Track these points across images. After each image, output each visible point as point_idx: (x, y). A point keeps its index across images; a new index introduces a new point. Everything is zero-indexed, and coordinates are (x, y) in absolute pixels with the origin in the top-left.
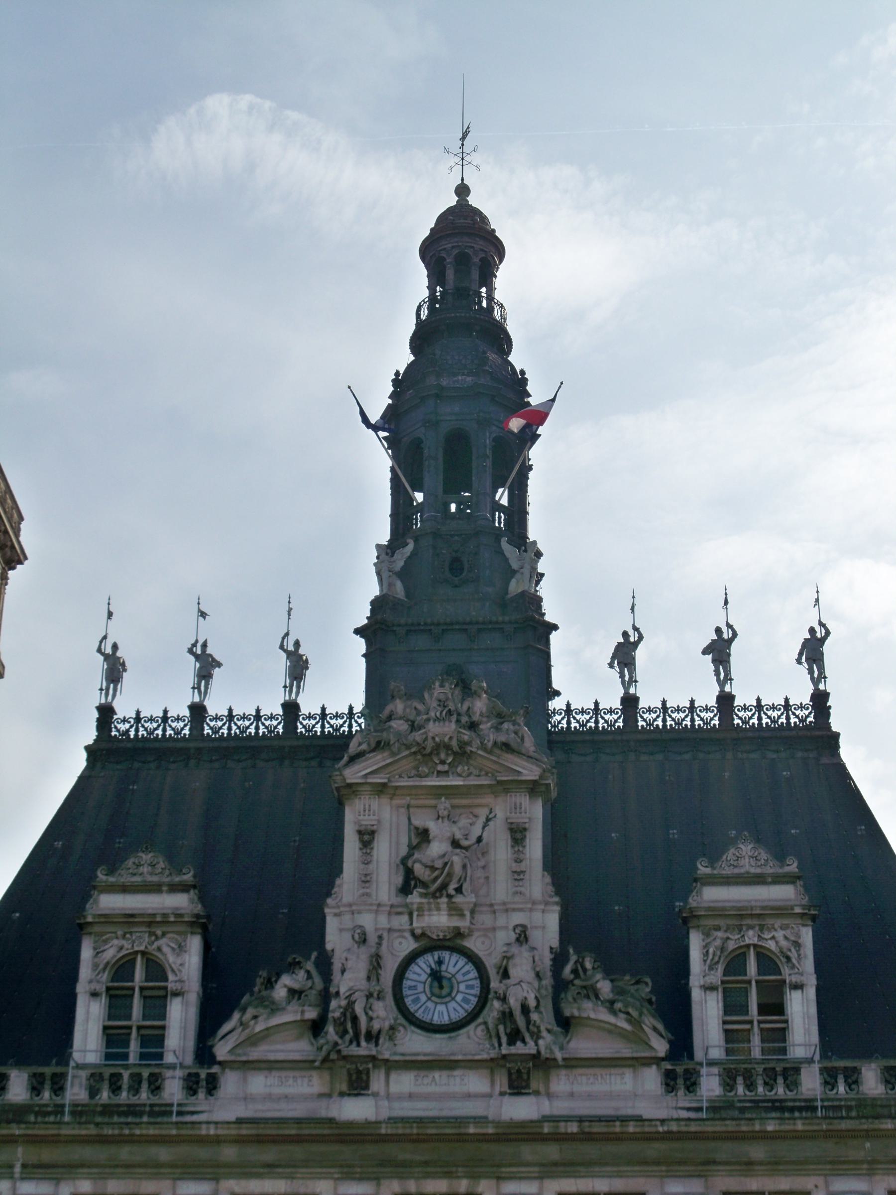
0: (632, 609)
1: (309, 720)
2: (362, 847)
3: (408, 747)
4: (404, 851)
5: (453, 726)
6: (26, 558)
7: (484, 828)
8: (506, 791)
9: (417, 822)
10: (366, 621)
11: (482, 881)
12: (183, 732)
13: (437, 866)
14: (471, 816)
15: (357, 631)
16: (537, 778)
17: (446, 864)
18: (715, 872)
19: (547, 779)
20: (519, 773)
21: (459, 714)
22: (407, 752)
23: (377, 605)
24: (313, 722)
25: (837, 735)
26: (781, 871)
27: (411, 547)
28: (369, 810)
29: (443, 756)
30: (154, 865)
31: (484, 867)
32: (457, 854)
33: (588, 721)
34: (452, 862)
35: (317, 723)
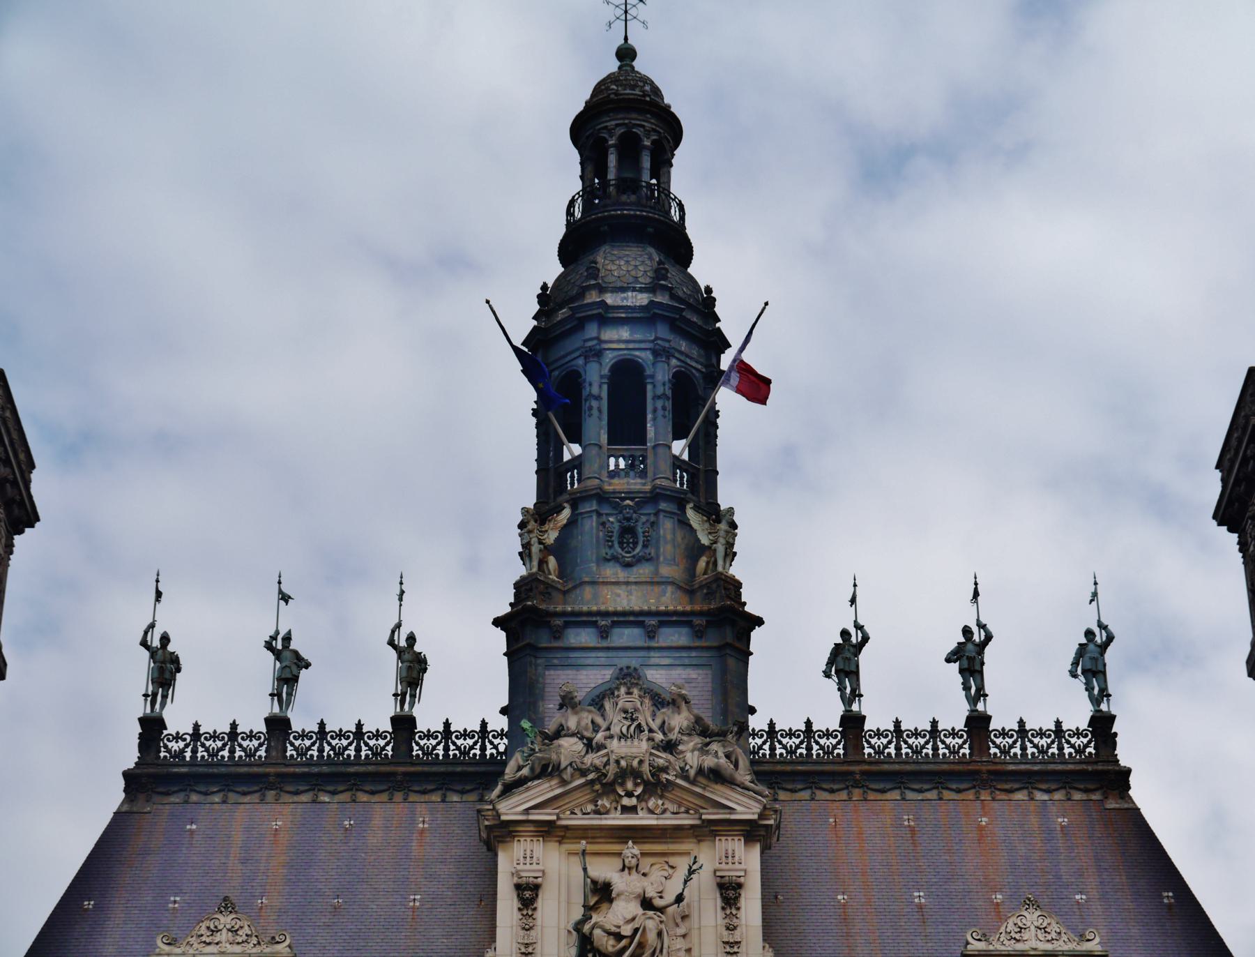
0: (853, 601)
1: (428, 740)
2: (520, 906)
3: (583, 773)
4: (578, 913)
5: (644, 745)
6: (38, 519)
7: (686, 882)
8: (714, 835)
10: (509, 609)
11: (682, 953)
12: (258, 754)
13: (623, 933)
14: (667, 867)
15: (497, 622)
16: (755, 817)
17: (636, 930)
18: (991, 948)
19: (769, 819)
21: (651, 731)
22: (581, 781)
23: (522, 588)
24: (434, 742)
25: (1128, 772)
26: (1079, 948)
27: (566, 513)
29: (630, 785)
30: (237, 930)
31: (684, 936)
32: (650, 918)
33: (798, 747)
34: (644, 929)
35: (438, 744)
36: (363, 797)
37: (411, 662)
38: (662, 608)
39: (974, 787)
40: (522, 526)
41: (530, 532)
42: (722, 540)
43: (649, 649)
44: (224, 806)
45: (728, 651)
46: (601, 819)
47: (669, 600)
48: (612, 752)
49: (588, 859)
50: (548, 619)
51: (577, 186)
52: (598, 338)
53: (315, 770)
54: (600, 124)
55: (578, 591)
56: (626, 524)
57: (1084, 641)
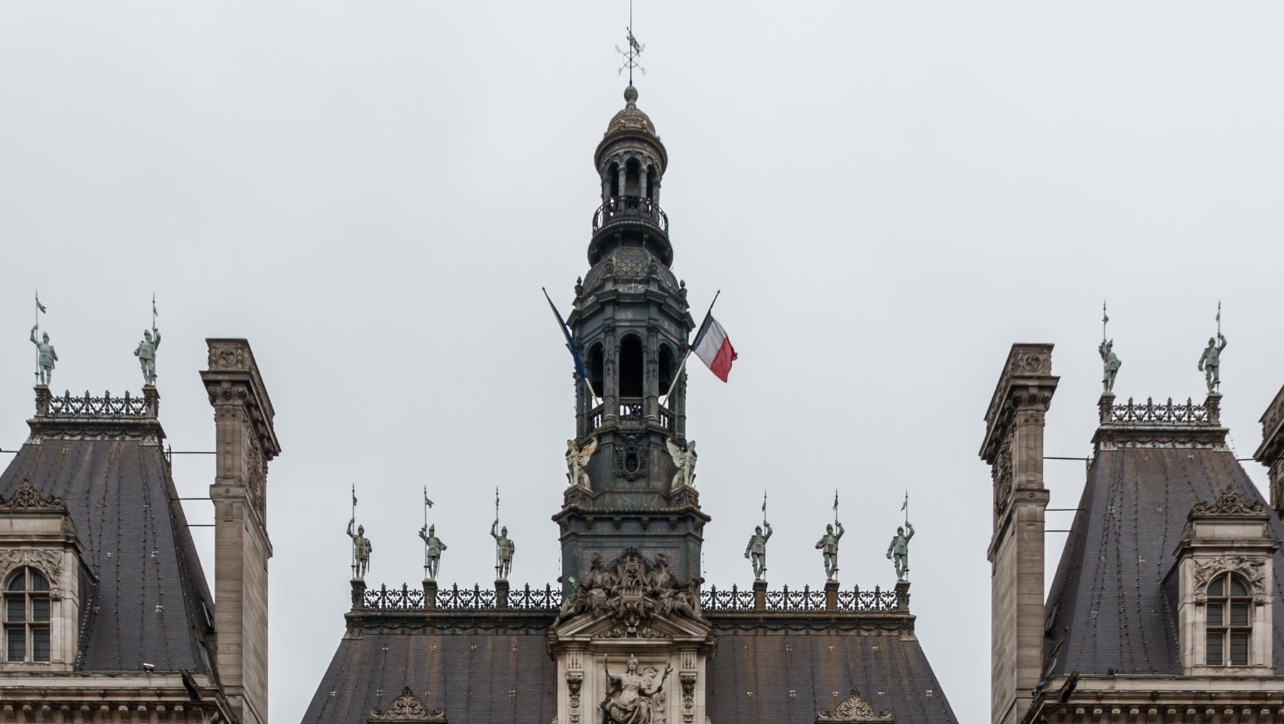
4: (603, 697)
7: (663, 679)
8: (680, 650)
9: (612, 673)
11: (661, 722)
13: (628, 709)
14: (653, 671)
17: (635, 708)
19: (710, 641)
20: (690, 636)
23: (570, 495)
27: (594, 444)
28: (577, 664)
31: (662, 712)
32: (643, 700)
34: (640, 707)
36: (480, 631)
37: (505, 546)
38: (652, 509)
39: (827, 628)
40: (568, 453)
41: (572, 457)
42: (687, 464)
43: (644, 536)
44: (403, 636)
45: (690, 538)
46: (615, 641)
47: (654, 504)
48: (622, 598)
49: (608, 665)
50: (584, 516)
51: (600, 202)
52: (613, 318)
53: (453, 614)
54: (614, 151)
55: (602, 498)
56: (630, 452)
57: (897, 535)
